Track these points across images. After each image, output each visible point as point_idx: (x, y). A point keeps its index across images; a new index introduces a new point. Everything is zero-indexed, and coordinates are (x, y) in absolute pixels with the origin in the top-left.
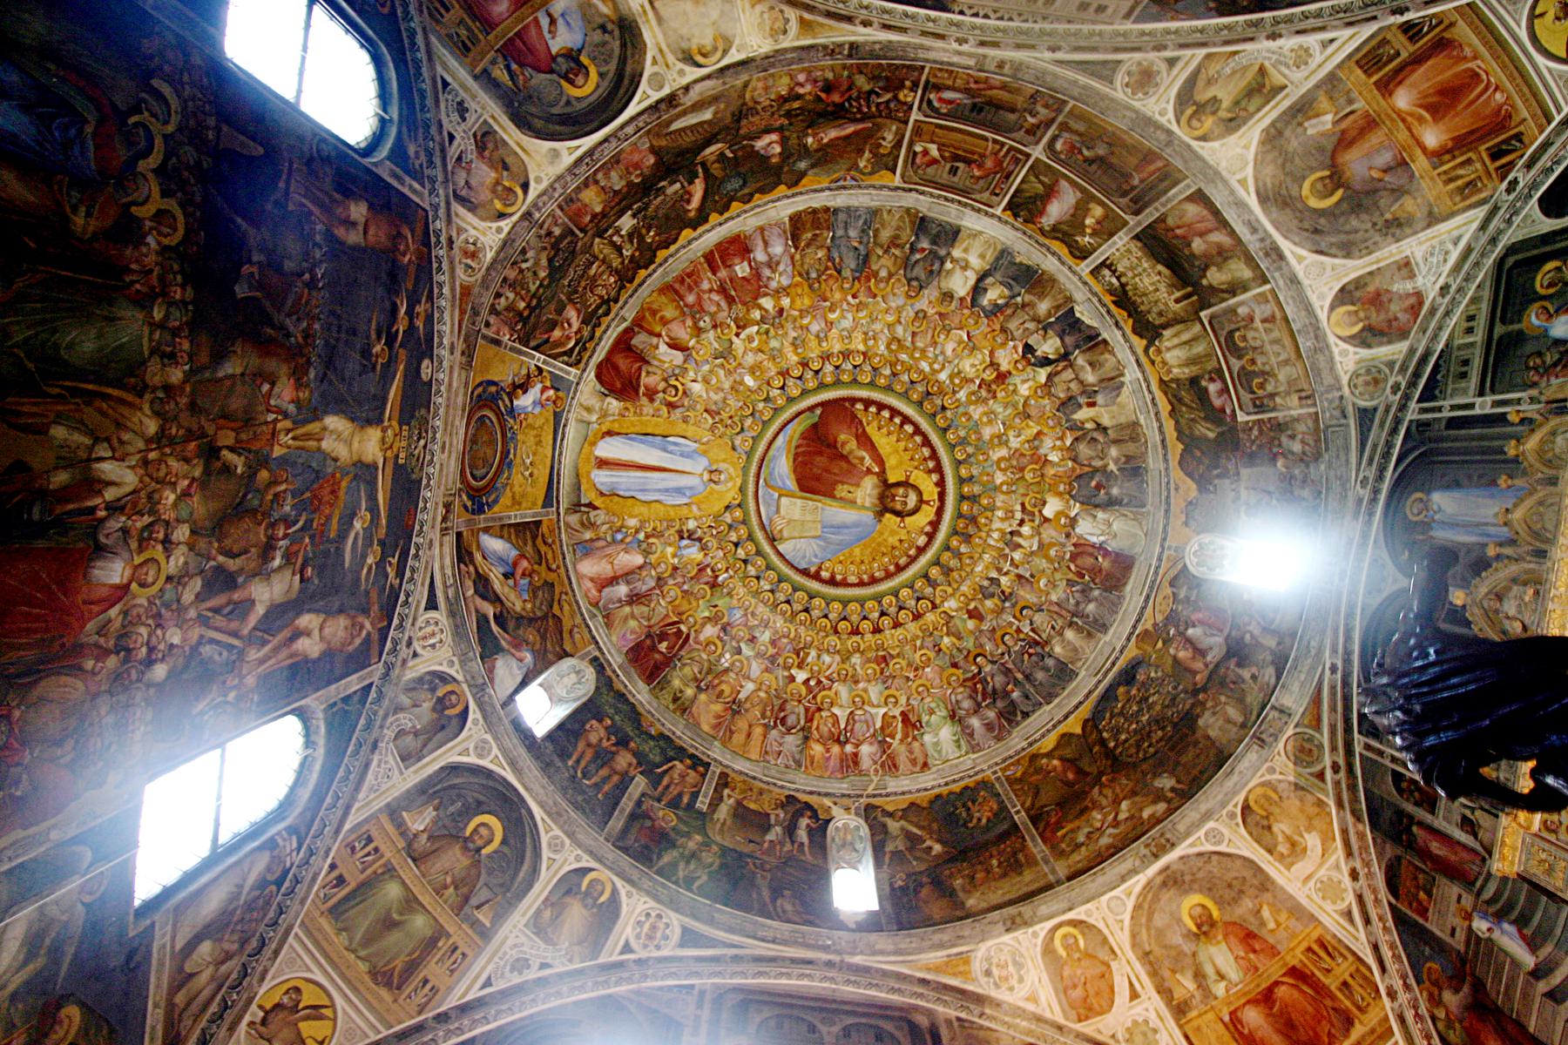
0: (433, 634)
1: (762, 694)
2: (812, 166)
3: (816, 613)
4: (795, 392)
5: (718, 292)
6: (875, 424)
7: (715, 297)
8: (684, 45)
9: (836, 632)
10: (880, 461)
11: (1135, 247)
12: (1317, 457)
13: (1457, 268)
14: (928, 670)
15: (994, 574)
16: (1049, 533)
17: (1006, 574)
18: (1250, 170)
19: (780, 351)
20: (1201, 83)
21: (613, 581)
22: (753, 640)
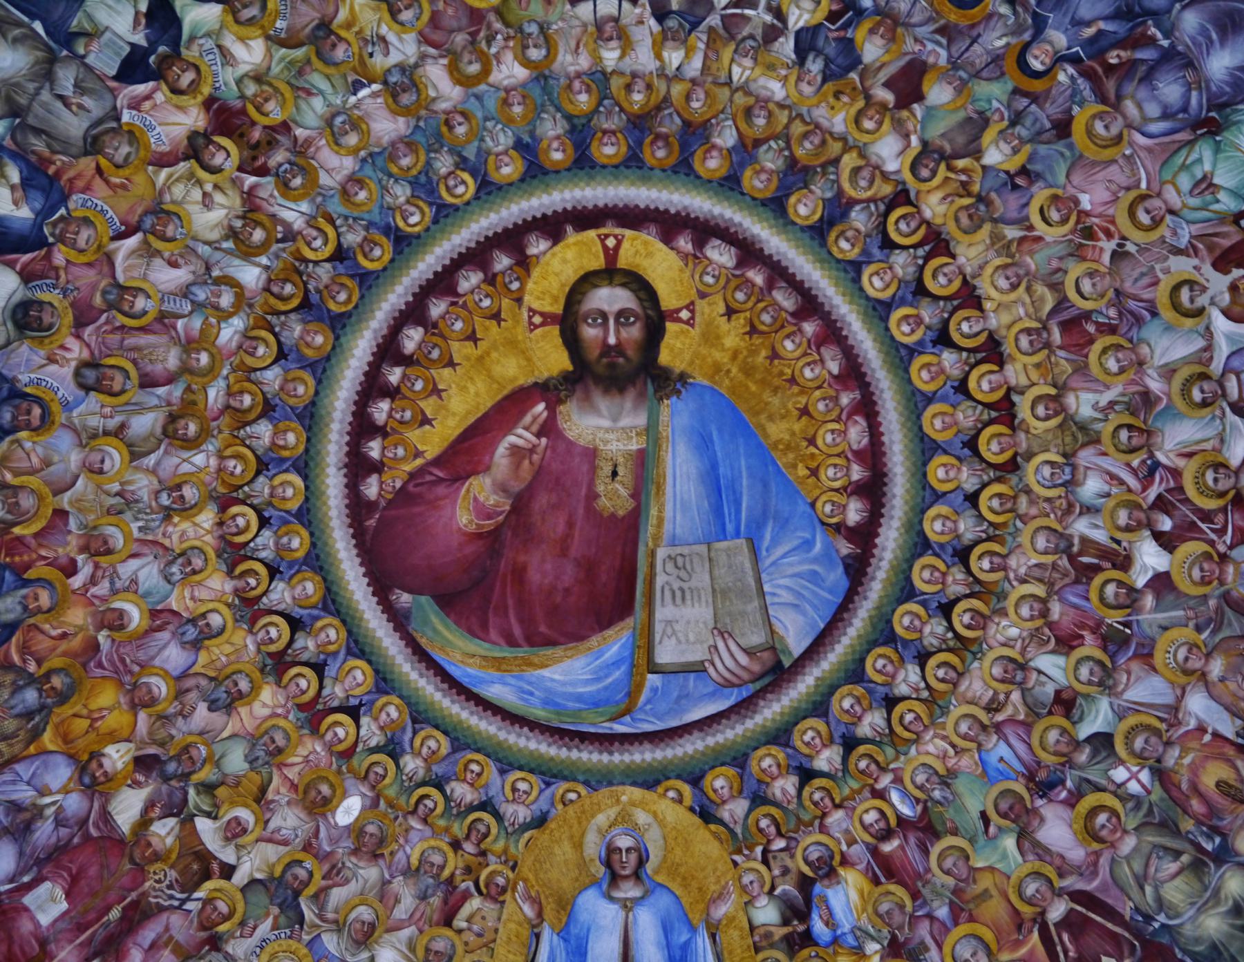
1: (1216, 668)
3: (967, 528)
4: (359, 675)
6: (414, 435)
9: (1012, 466)
10: (512, 405)
14: (1086, 204)
15: (786, 47)
17: (779, 14)
19: (253, 740)
22: (1066, 703)
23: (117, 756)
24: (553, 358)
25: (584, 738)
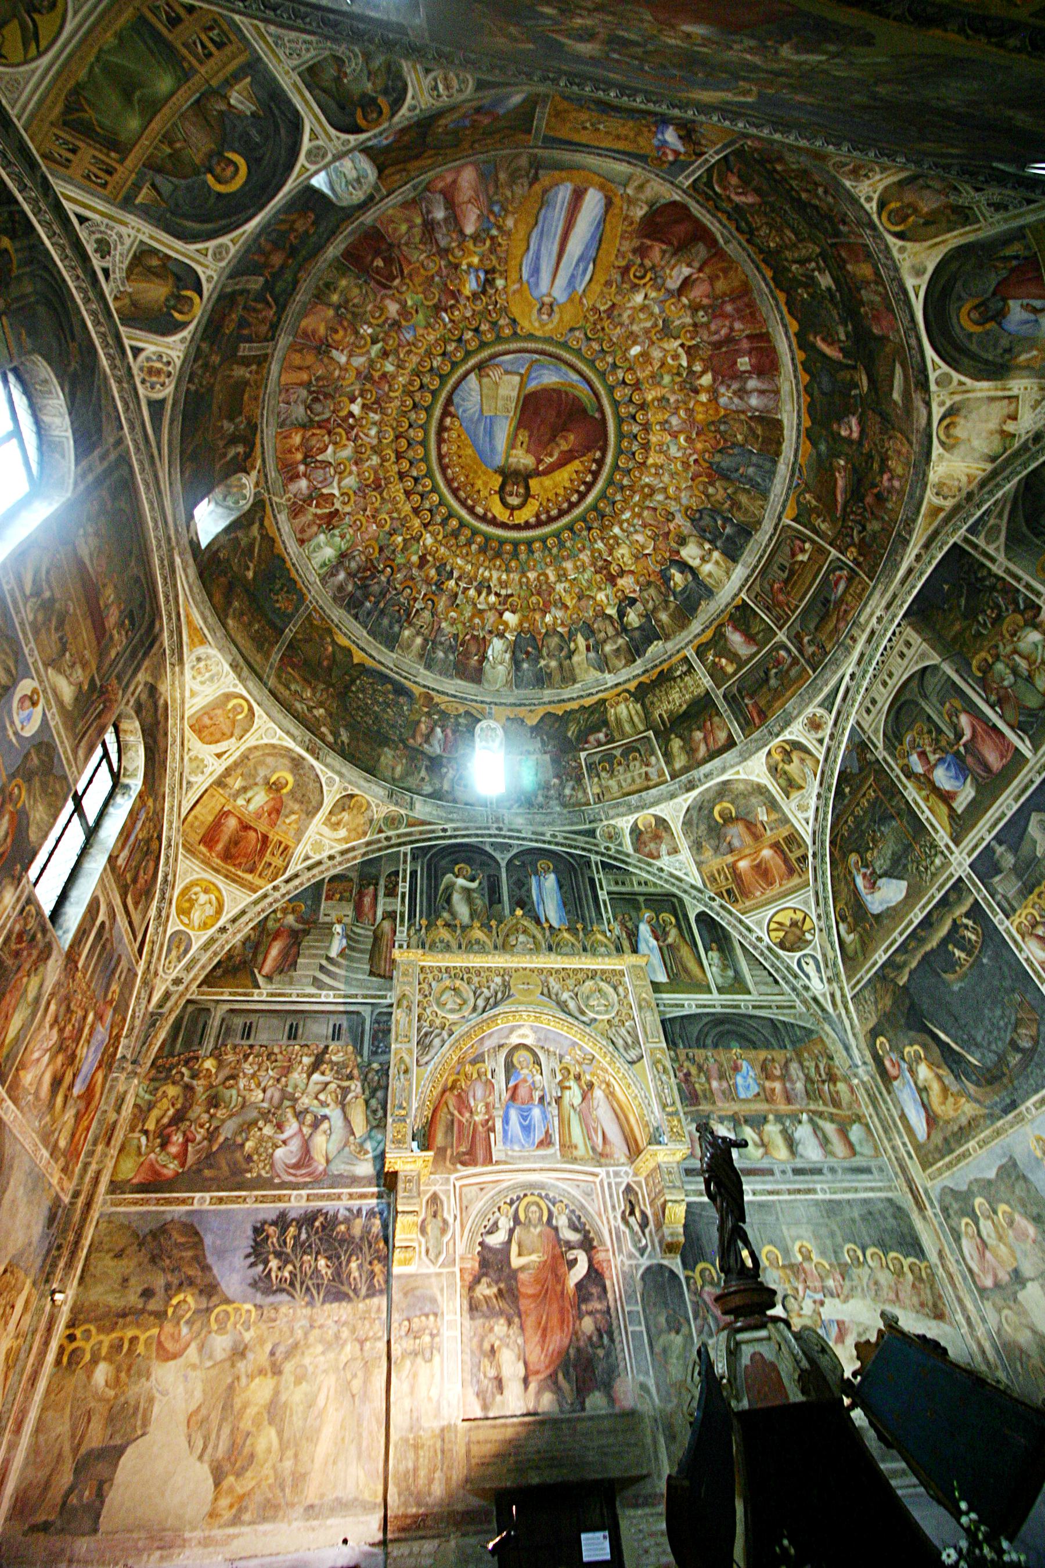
0: (448, 87)
2: (819, 455)
3: (413, 416)
4: (618, 395)
5: (728, 336)
7: (723, 332)
8: (963, 412)
9: (397, 437)
11: (701, 691)
12: (564, 805)
13: (671, 875)
15: (456, 574)
16: (491, 617)
18: (743, 776)
19: (659, 384)
20: (803, 755)
21: (451, 204)
22: (385, 354)
23: (704, 397)
24: (533, 483)
25: (550, 355)
